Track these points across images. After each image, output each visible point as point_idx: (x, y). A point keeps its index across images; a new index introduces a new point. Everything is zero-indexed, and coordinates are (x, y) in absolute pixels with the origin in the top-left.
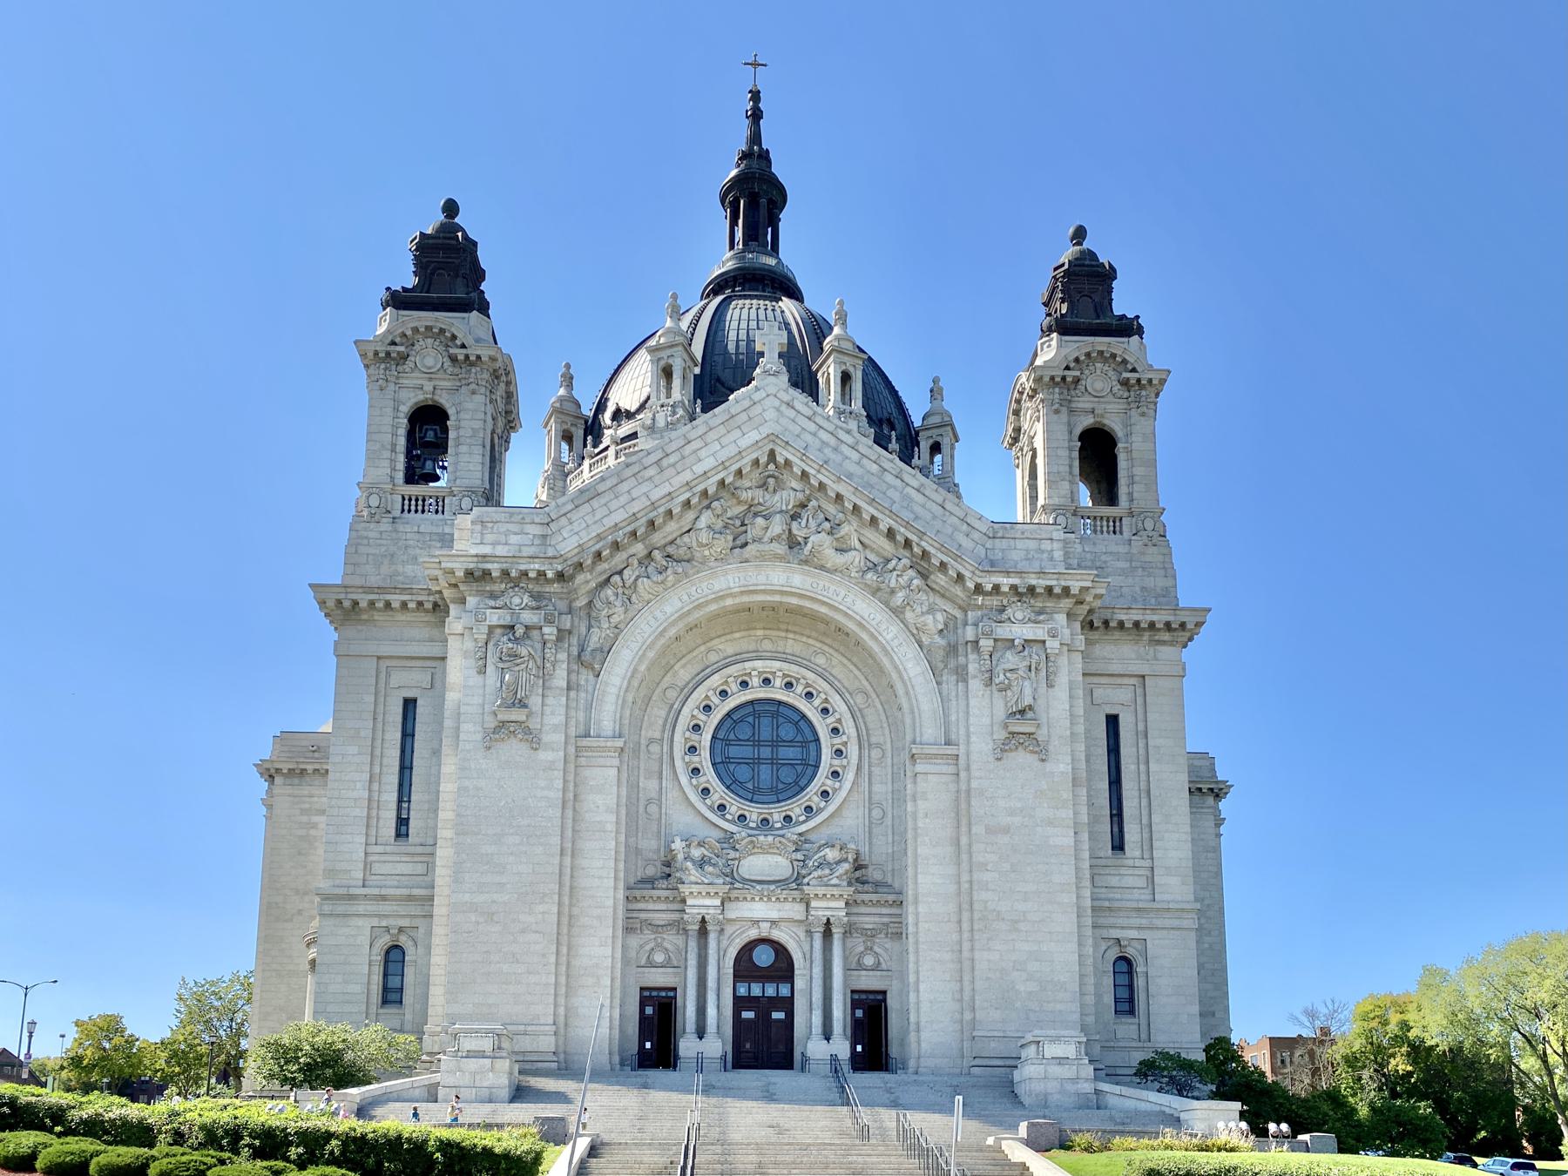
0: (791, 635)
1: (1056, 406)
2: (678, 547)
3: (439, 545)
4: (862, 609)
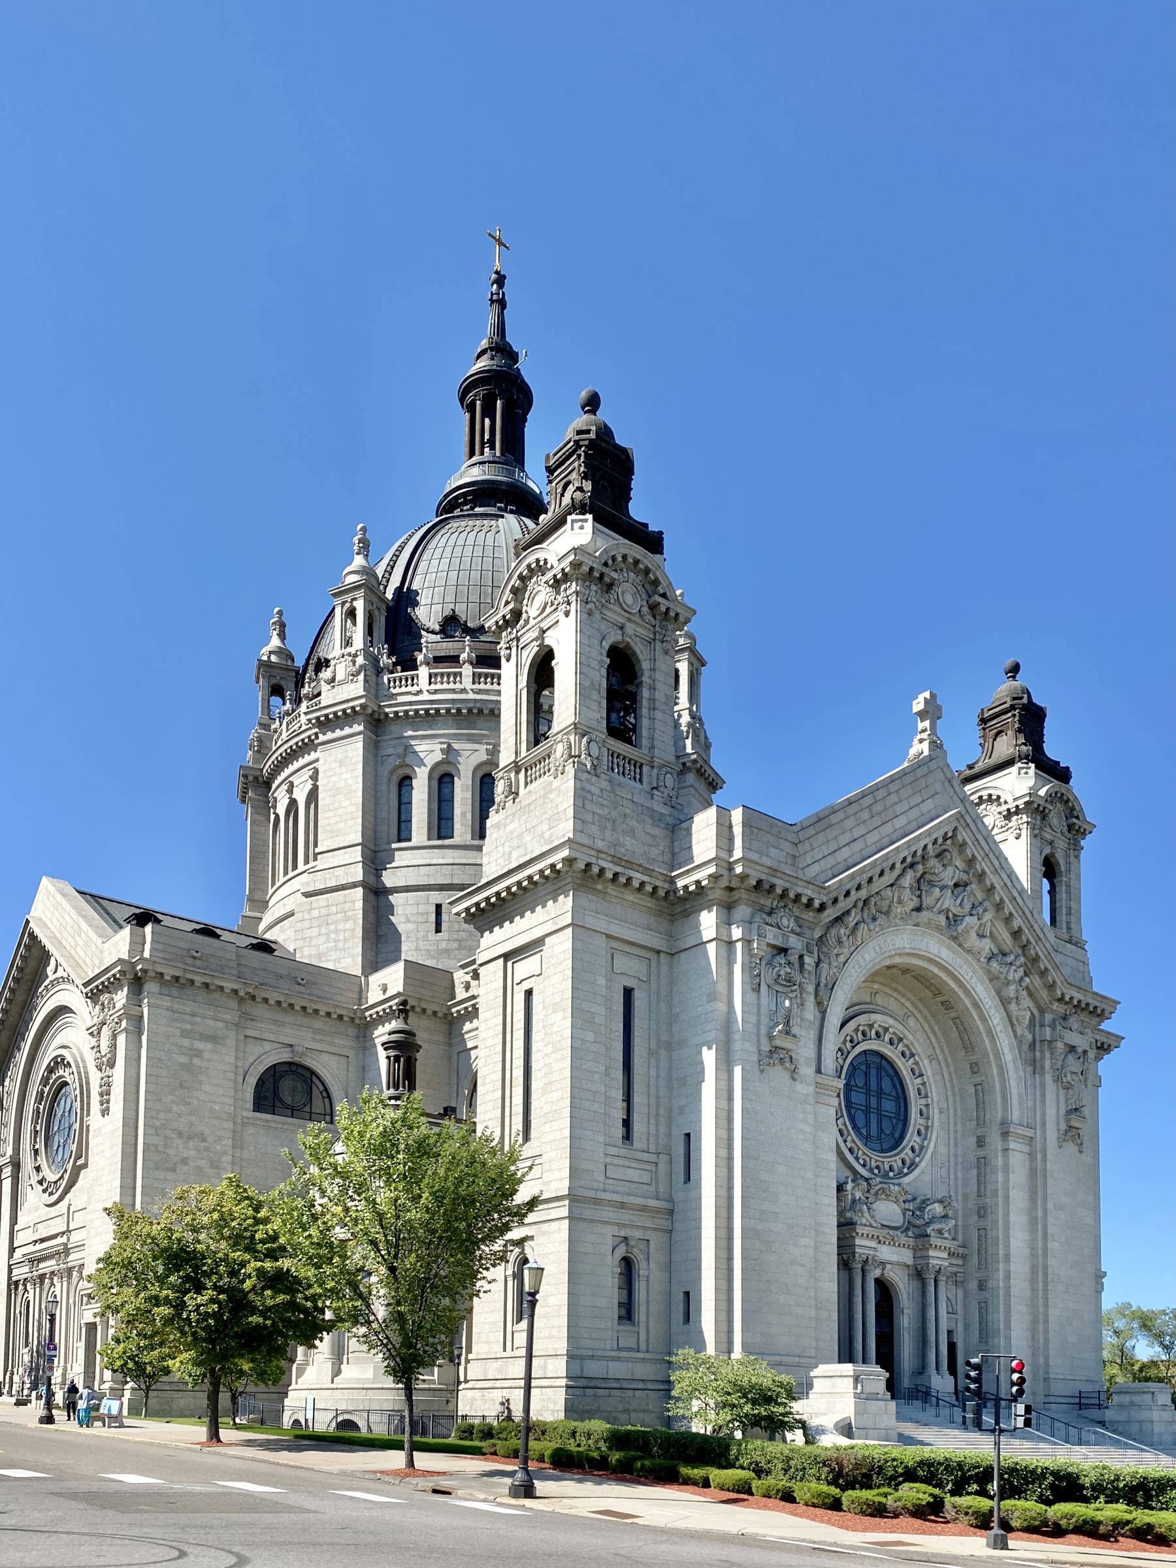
0: (895, 995)
1: (1036, 832)
2: (882, 899)
3: (650, 821)
4: (983, 992)
